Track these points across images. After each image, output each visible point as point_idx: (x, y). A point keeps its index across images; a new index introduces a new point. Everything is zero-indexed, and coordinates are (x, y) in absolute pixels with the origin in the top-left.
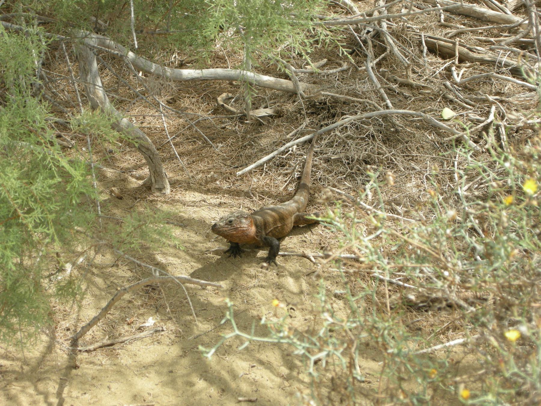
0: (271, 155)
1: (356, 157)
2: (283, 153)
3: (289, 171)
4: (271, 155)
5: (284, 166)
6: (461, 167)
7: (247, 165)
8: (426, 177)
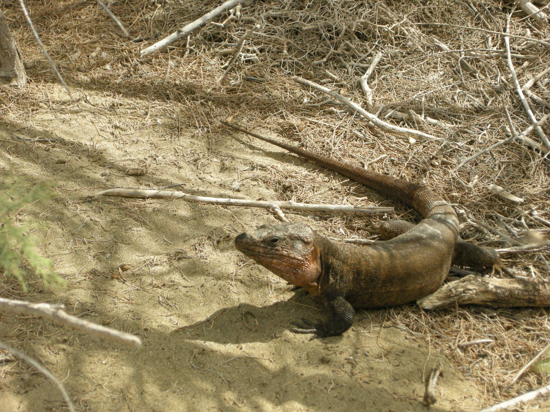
0: (198, 22)
1: (345, 27)
2: (219, 18)
3: (229, 50)
4: (198, 22)
5: (220, 40)
6: (516, 47)
7: (157, 38)
8: (462, 62)
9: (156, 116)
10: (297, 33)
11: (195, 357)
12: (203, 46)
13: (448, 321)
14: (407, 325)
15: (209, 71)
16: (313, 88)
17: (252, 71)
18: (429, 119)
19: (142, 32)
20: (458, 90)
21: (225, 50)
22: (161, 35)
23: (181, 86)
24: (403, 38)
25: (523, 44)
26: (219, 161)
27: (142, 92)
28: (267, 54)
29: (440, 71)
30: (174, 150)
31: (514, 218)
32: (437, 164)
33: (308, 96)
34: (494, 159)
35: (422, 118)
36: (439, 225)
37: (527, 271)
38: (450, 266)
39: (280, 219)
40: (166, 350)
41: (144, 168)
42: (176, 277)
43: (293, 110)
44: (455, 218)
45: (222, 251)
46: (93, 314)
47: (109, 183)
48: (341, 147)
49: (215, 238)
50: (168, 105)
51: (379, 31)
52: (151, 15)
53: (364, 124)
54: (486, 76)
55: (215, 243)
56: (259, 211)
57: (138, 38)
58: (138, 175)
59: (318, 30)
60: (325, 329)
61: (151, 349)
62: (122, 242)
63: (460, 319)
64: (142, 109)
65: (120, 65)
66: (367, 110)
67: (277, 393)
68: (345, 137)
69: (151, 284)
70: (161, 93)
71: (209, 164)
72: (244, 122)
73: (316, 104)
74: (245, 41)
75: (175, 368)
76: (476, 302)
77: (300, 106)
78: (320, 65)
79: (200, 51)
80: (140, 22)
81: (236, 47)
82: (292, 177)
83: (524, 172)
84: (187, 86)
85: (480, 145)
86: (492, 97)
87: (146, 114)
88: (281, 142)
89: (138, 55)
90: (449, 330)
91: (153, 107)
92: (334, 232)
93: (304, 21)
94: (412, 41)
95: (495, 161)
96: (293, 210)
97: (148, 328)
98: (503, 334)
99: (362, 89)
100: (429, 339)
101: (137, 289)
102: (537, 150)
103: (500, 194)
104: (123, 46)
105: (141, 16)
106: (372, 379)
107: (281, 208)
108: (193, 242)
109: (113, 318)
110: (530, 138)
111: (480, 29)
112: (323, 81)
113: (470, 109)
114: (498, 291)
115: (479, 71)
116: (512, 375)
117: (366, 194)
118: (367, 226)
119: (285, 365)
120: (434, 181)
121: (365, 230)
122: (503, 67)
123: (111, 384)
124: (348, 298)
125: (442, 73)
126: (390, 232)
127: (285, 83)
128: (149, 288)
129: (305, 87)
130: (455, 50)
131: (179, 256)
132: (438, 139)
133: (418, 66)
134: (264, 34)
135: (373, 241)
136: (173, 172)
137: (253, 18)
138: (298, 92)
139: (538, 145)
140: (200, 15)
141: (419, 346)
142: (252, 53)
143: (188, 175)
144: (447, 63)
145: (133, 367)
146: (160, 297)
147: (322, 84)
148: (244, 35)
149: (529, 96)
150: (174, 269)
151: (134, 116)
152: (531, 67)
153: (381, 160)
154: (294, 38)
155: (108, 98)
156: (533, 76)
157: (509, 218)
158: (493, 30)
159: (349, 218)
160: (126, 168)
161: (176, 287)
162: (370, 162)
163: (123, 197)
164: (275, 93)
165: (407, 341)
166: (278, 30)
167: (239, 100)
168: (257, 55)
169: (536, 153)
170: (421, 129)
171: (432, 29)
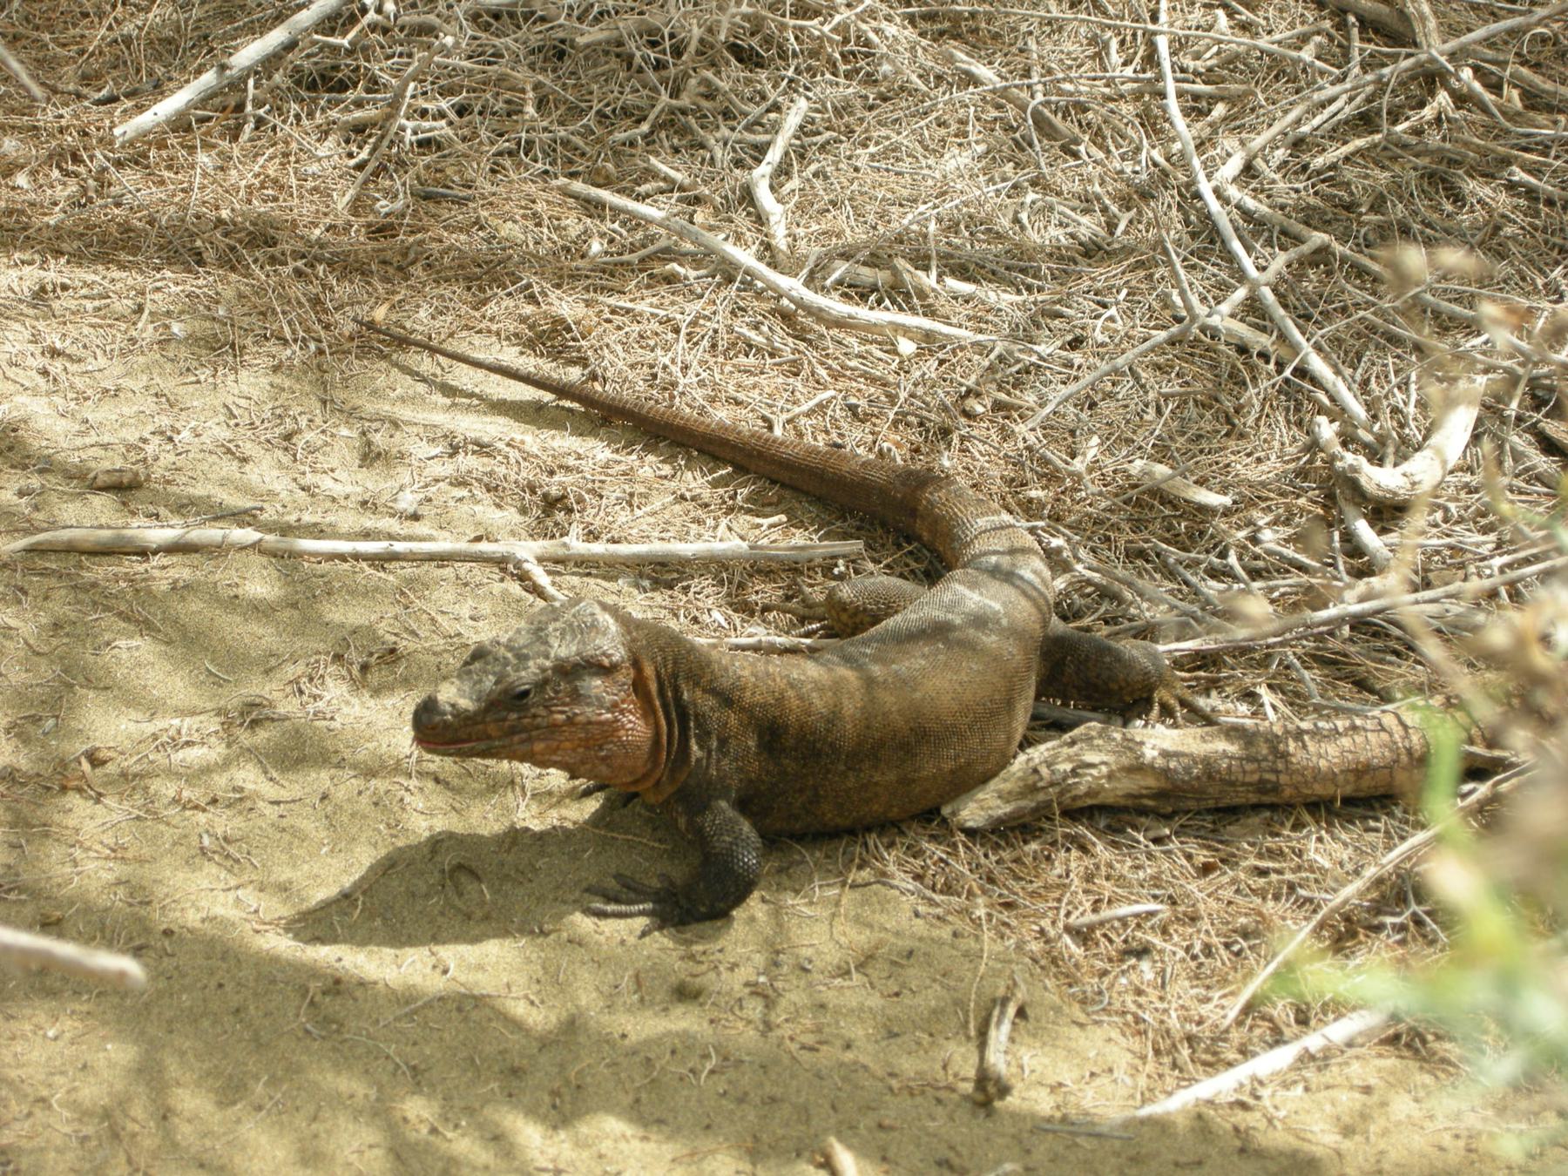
0: (276, 37)
1: (697, 32)
3: (369, 113)
4: (276, 37)
5: (343, 87)
7: (160, 89)
8: (1036, 114)
9: (168, 313)
10: (561, 55)
11: (312, 1003)
12: (295, 107)
13: (1035, 859)
14: (918, 877)
15: (313, 173)
16: (616, 211)
17: (437, 171)
18: (952, 283)
19: (115, 73)
20: (1031, 196)
21: (358, 114)
22: (170, 79)
23: (235, 224)
24: (867, 55)
25: (1208, 55)
26: (355, 434)
27: (123, 248)
28: (478, 119)
29: (977, 142)
30: (224, 411)
31: (1208, 552)
32: (980, 409)
33: (602, 235)
34: (1143, 386)
35: (929, 280)
36: (995, 586)
37: (1252, 704)
38: (1031, 701)
39: (537, 591)
40: (228, 988)
41: (140, 468)
42: (249, 777)
43: (561, 277)
44: (1038, 563)
45: (376, 692)
46: (12, 896)
47: (40, 516)
48: (704, 375)
49: (355, 657)
50: (201, 282)
51: (797, 38)
52: (140, 23)
53: (766, 306)
54: (1108, 152)
55: (355, 670)
56: (478, 573)
57: (104, 92)
58: (124, 488)
59: (620, 44)
60: (683, 902)
61: (184, 989)
62: (89, 683)
63: (1068, 850)
64: (127, 297)
65: (56, 173)
66: (773, 265)
67: (555, 1093)
68: (714, 346)
69: (175, 801)
70: (180, 246)
71: (326, 444)
72: (422, 319)
73: (626, 257)
74: (412, 85)
75: (256, 1039)
76: (1110, 800)
77: (580, 263)
78: (632, 144)
79: (284, 122)
80: (110, 45)
81: (389, 105)
82: (568, 469)
83: (1229, 421)
84: (253, 224)
85: (1101, 351)
86: (1129, 209)
87: (140, 309)
88: (532, 369)
89: (107, 142)
90: (1038, 884)
91: (158, 289)
92: (695, 620)
93: (579, 19)
94: (892, 62)
95: (1146, 392)
96: (576, 565)
97: (176, 929)
98: (1192, 887)
99: (754, 206)
100: (981, 912)
101: (138, 818)
102: (1264, 356)
103: (1164, 486)
104: (61, 116)
105: (110, 28)
106: (823, 1037)
107: (540, 560)
108: (291, 671)
109: (72, 903)
110: (1242, 320)
111: (1084, 16)
112: (643, 189)
113: (1067, 249)
114: (1172, 765)
115: (1087, 138)
116: (1224, 1002)
117: (782, 507)
118: (788, 598)
119: (574, 1010)
120: (974, 458)
121: (784, 612)
122: (1153, 123)
123: (73, 1096)
124: (743, 805)
125: (981, 148)
126: (857, 611)
127: (534, 202)
128: (173, 811)
129: (592, 210)
130: (1017, 82)
131: (254, 715)
132: (980, 337)
133: (913, 132)
134: (466, 64)
135: (808, 641)
136: (223, 473)
137: (432, 18)
138: (573, 225)
139: (1264, 341)
140: (279, 18)
141: (955, 935)
142: (434, 119)
143: (267, 479)
144: (996, 119)
145: (136, 1042)
146: (205, 837)
147: (641, 198)
148: (411, 69)
149: (1234, 202)
150: (242, 754)
151: (104, 318)
152: (1235, 119)
153: (822, 407)
154: (554, 70)
155: (27, 269)
156: (1242, 143)
157: (1193, 555)
158: (1122, 19)
159: (735, 578)
160: (89, 470)
161: (248, 804)
162: (789, 416)
163: (83, 553)
164: (508, 230)
165: (919, 921)
166: (508, 49)
167: (405, 255)
168: (450, 123)
169: (1261, 363)
170: (930, 312)
171: (947, 25)
